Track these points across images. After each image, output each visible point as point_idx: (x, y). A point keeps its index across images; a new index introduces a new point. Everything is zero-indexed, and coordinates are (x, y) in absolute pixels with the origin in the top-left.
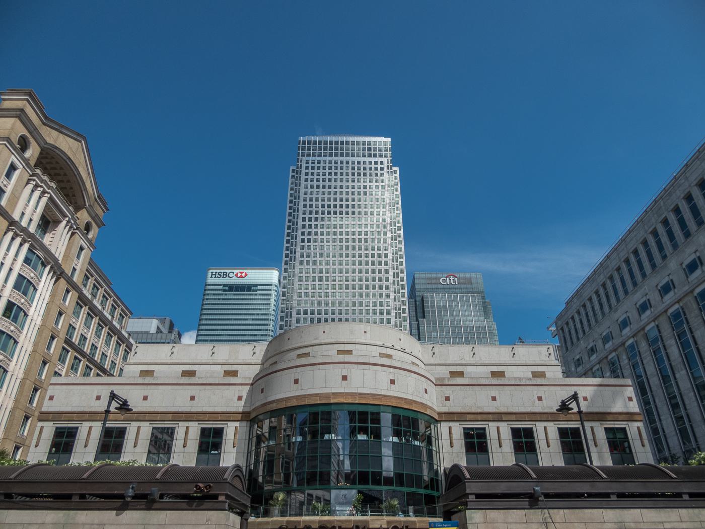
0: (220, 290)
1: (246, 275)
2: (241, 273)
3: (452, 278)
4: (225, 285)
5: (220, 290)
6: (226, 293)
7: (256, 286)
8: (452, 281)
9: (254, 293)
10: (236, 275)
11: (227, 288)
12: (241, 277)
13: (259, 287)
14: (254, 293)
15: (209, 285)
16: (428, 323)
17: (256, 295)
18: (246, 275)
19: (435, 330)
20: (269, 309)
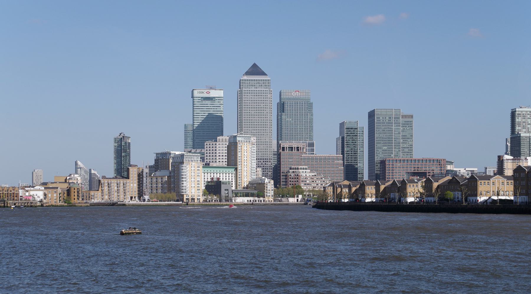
0: (200, 100)
1: (210, 93)
2: (208, 92)
3: (297, 93)
4: (202, 98)
5: (200, 100)
6: (203, 101)
7: (214, 98)
8: (297, 94)
9: (214, 101)
10: (206, 92)
11: (203, 99)
12: (208, 93)
13: (216, 99)
14: (214, 101)
15: (195, 97)
16: (285, 115)
17: (215, 102)
18: (210, 93)
19: (288, 117)
20: (221, 109)
